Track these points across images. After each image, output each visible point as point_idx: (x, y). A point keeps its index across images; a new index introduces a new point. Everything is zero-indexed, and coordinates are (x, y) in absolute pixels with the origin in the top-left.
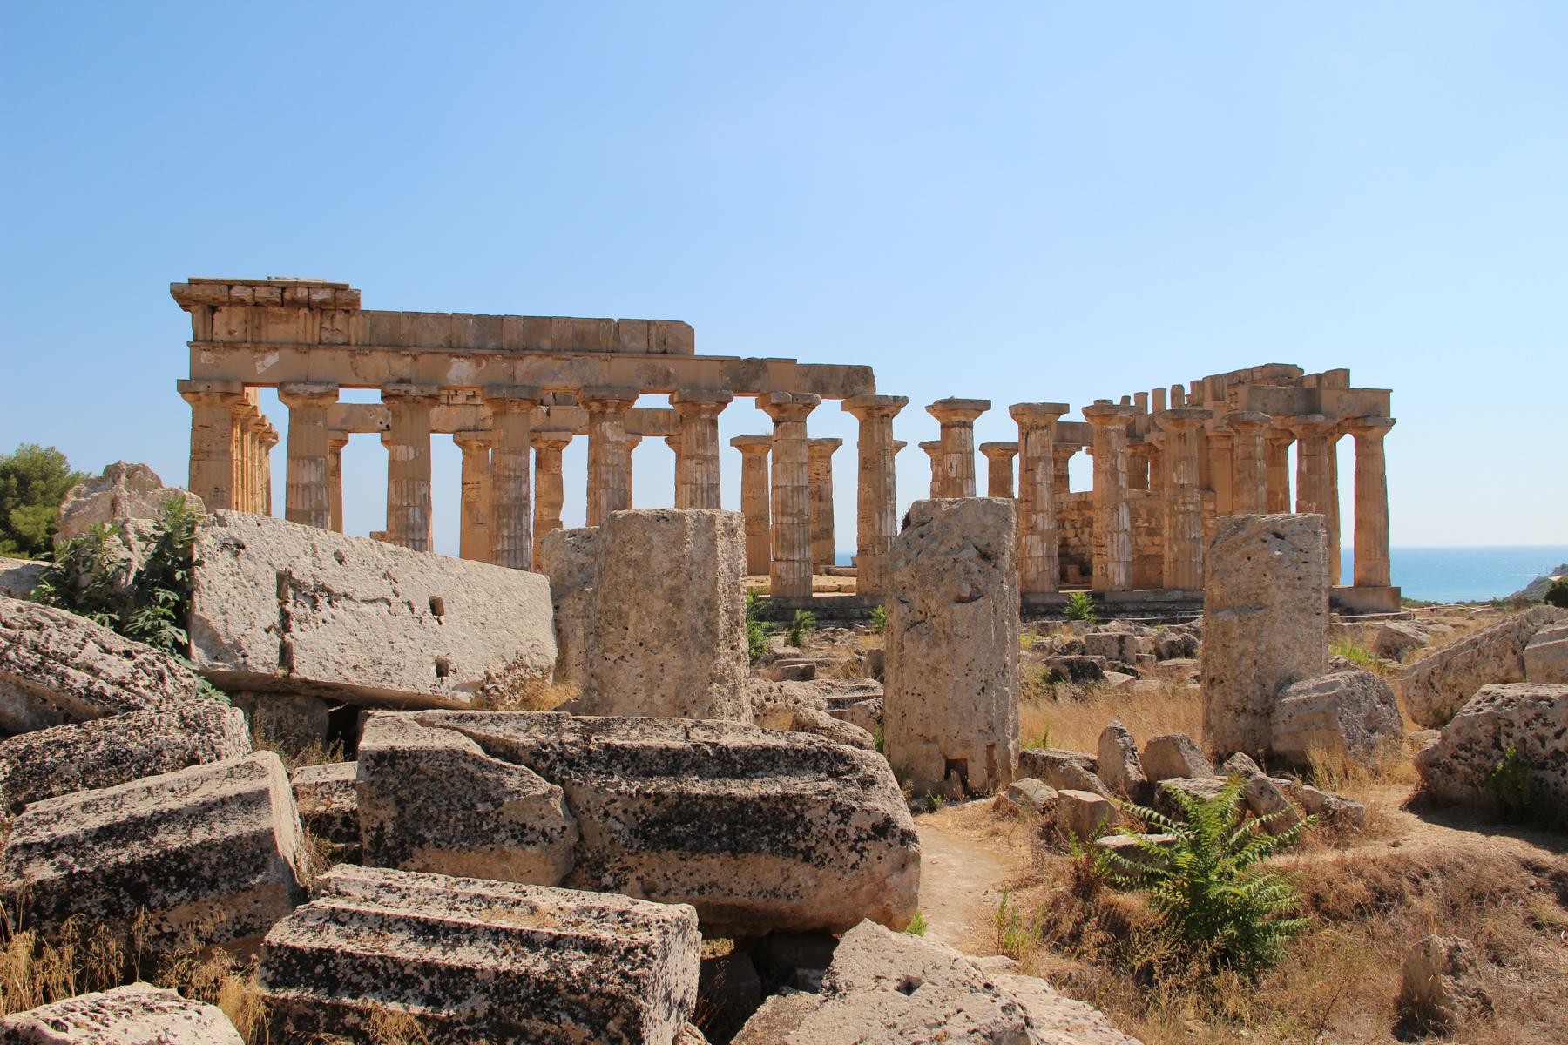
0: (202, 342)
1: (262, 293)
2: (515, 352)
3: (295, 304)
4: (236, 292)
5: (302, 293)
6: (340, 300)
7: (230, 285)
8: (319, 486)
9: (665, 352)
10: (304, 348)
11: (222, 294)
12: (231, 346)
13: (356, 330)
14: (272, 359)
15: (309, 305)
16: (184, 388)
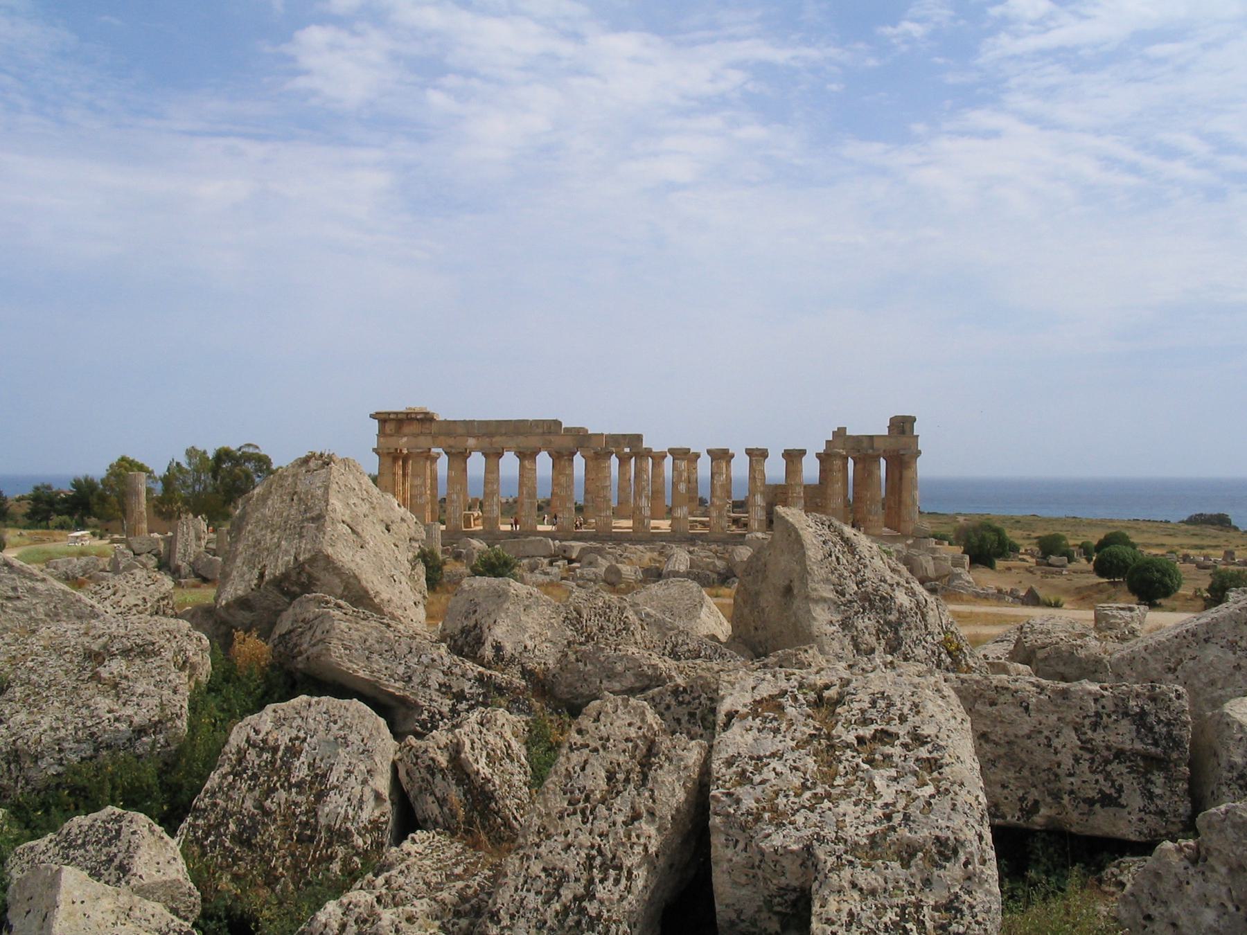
0: (382, 433)
1: (400, 416)
2: (491, 435)
3: (412, 419)
4: (392, 416)
5: (413, 416)
6: (427, 418)
7: (389, 414)
8: (421, 486)
9: (550, 433)
10: (416, 435)
11: (387, 416)
12: (391, 435)
13: (434, 428)
14: (405, 439)
15: (418, 420)
16: (374, 450)
